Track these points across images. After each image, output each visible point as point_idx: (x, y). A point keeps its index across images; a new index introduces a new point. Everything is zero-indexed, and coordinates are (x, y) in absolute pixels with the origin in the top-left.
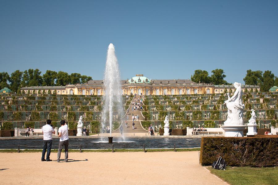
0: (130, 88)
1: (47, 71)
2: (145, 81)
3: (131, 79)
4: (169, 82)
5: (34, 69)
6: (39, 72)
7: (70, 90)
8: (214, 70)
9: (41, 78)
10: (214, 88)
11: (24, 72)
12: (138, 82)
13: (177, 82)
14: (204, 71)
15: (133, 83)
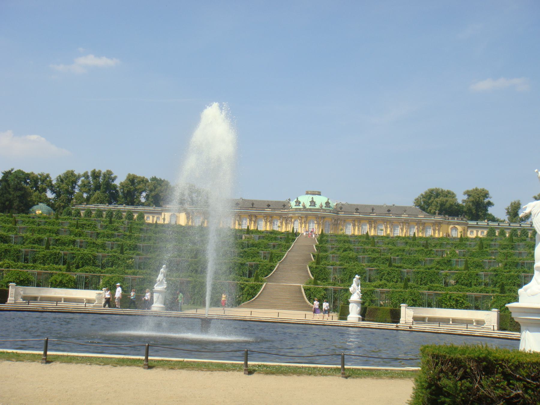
0: (291, 218)
1: (129, 175)
2: (324, 205)
3: (296, 200)
4: (373, 210)
5: (104, 171)
6: (113, 176)
7: (171, 216)
8: (470, 188)
9: (115, 187)
10: (466, 227)
11: (84, 176)
12: (310, 207)
13: (389, 211)
14: (449, 192)
15: (299, 207)
